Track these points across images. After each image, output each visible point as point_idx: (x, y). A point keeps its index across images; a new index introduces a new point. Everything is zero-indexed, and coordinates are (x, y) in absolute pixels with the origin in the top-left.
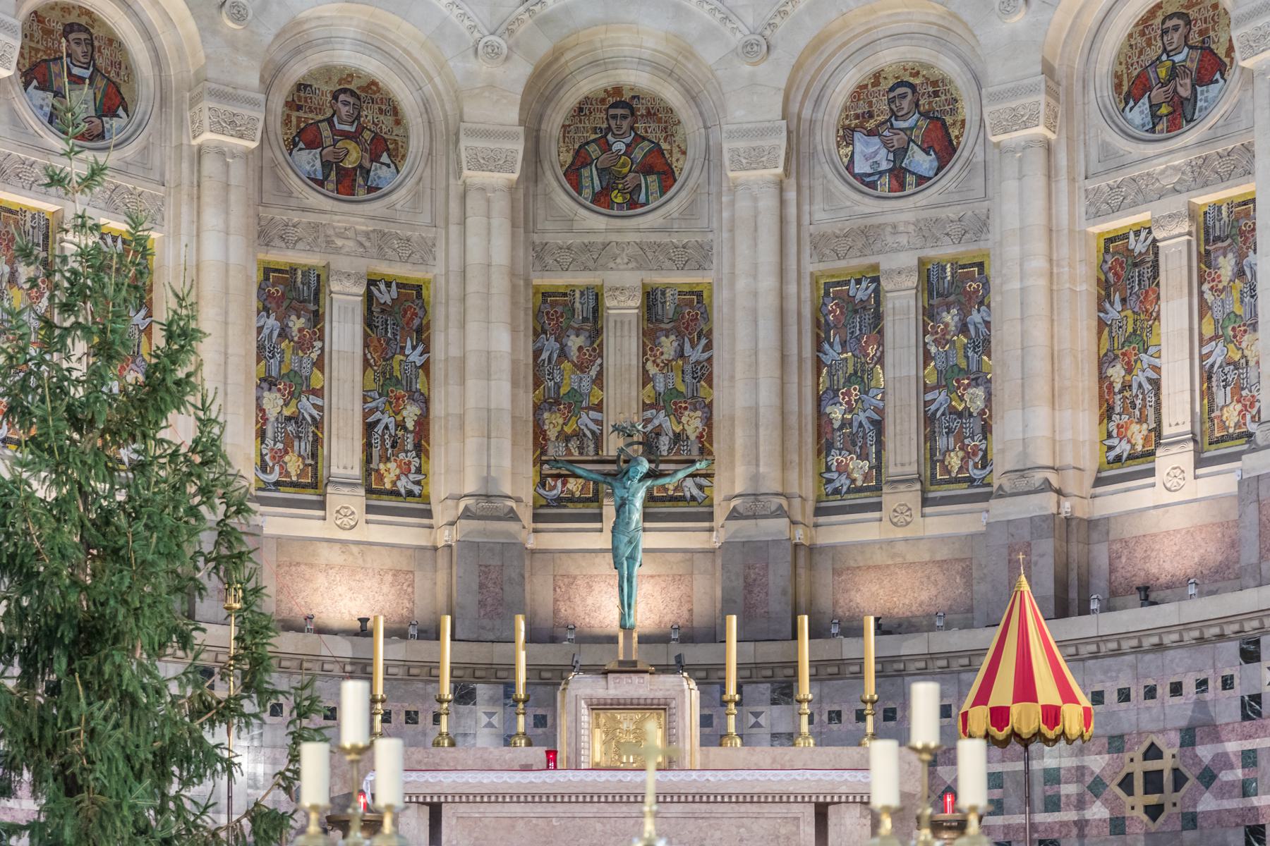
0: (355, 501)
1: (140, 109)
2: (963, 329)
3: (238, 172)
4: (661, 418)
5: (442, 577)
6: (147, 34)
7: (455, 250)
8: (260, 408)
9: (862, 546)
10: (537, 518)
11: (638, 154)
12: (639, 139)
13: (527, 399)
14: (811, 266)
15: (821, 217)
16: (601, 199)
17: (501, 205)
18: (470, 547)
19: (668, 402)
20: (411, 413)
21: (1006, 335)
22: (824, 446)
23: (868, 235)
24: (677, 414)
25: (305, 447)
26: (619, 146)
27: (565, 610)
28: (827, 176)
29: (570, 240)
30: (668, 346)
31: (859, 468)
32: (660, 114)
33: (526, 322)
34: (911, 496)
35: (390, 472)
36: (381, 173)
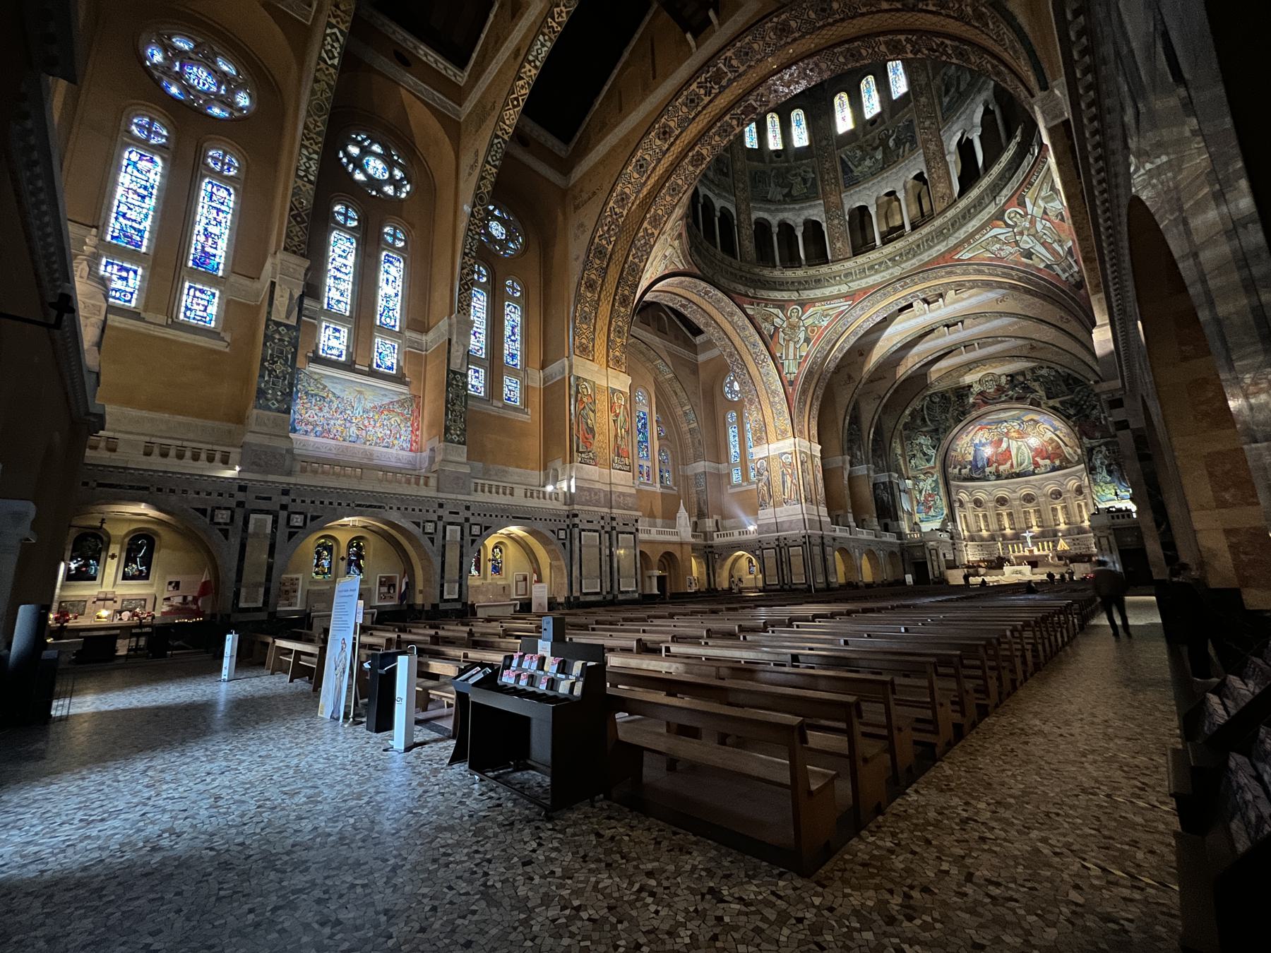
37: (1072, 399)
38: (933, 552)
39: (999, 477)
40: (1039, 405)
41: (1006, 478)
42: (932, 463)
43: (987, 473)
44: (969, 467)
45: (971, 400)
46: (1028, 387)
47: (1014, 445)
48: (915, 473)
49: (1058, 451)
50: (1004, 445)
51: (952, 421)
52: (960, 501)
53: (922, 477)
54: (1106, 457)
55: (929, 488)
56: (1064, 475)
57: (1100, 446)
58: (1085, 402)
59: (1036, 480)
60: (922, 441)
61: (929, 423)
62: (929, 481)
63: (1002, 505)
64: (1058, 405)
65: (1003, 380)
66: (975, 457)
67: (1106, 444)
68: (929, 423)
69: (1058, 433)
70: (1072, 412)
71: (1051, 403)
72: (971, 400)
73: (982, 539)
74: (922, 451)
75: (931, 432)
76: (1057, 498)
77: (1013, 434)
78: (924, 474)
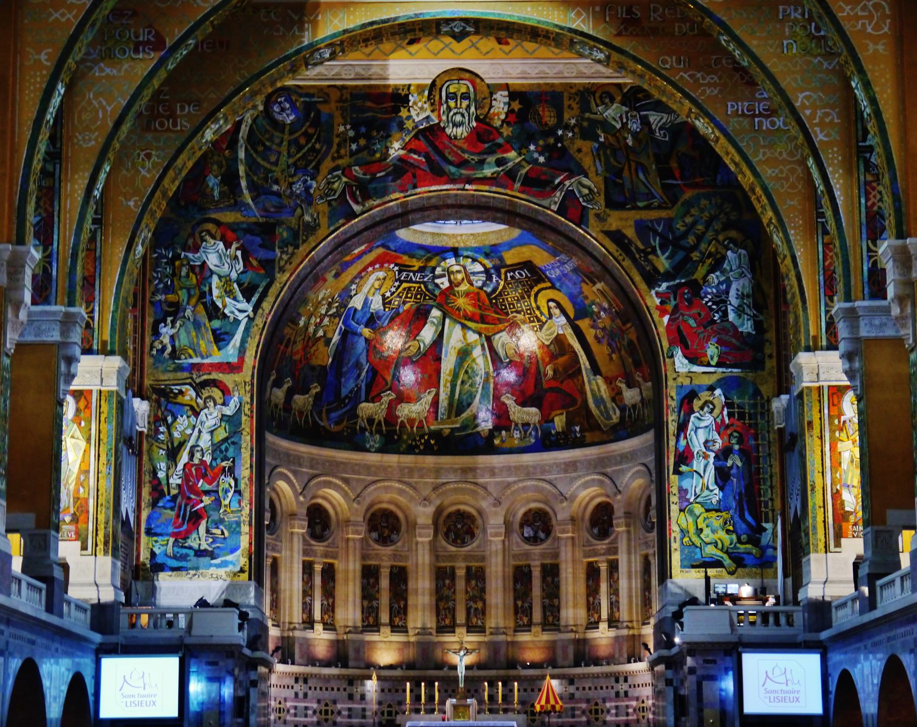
1: (332, 528)
2: (553, 582)
3: (358, 545)
4: (471, 604)
5: (411, 651)
7: (414, 558)
8: (362, 605)
9: (526, 642)
10: (437, 632)
11: (465, 528)
12: (465, 524)
14: (513, 563)
15: (516, 550)
17: (427, 547)
18: (418, 643)
19: (473, 599)
20: (402, 604)
22: (516, 613)
23: (527, 555)
24: (475, 602)
25: (374, 615)
26: (459, 526)
27: (445, 659)
28: (516, 537)
29: (446, 554)
31: (525, 620)
33: (434, 577)
34: (539, 629)
35: (397, 620)
36: (394, 537)
37: (669, 223)
40: (581, 220)
42: (230, 353)
45: (396, 149)
46: (564, 150)
49: (567, 386)
51: (322, 206)
54: (720, 428)
55: (206, 437)
56: (572, 466)
57: (711, 388)
58: (700, 238)
59: (492, 472)
60: (212, 260)
62: (211, 417)
63: (384, 540)
64: (630, 233)
65: (500, 105)
67: (726, 384)
68: (248, 198)
69: (584, 324)
70: (663, 262)
71: (616, 220)
72: (396, 149)
73: (312, 661)
74: (204, 296)
75: (250, 230)
78: (199, 387)
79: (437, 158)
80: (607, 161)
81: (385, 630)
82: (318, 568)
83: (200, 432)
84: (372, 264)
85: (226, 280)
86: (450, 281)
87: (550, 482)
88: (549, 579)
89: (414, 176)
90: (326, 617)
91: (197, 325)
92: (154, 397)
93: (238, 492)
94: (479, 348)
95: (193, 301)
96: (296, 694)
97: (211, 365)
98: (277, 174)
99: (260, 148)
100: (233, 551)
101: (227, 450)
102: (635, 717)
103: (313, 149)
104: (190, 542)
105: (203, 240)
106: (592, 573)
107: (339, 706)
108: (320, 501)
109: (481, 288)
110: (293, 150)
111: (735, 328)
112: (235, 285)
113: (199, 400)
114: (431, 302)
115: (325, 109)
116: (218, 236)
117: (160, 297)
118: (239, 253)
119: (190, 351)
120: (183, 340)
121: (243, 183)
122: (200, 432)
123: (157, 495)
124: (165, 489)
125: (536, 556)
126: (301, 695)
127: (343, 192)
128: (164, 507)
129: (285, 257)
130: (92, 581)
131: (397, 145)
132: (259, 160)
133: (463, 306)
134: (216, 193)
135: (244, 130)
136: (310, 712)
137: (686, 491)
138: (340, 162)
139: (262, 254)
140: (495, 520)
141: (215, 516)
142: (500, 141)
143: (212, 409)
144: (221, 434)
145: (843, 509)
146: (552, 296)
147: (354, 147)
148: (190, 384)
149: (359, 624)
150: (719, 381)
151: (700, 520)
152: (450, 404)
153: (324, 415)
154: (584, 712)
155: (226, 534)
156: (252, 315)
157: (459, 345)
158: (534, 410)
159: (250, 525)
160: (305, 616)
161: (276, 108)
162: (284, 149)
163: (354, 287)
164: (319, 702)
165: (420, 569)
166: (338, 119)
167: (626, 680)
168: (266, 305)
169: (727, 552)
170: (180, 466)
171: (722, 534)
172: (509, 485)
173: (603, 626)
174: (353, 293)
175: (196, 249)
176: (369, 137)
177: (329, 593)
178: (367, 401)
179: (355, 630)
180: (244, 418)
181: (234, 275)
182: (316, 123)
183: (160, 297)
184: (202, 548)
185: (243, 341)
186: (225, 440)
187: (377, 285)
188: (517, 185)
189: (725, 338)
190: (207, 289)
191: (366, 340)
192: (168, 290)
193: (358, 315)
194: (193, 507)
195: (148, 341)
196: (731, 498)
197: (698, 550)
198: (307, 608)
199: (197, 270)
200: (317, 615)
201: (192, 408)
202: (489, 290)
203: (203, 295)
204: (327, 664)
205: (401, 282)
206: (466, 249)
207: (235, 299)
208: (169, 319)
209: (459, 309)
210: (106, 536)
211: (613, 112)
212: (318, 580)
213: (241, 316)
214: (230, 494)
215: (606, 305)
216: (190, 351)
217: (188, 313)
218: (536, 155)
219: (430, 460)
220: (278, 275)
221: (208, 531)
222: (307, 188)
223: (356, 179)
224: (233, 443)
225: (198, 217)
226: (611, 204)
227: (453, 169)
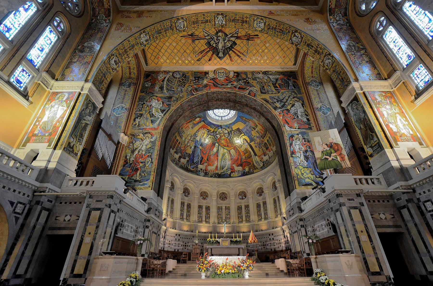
0: (205, 222)
6: (191, 189)
13: (217, 214)
16: (222, 200)
17: (215, 200)
18: (213, 226)
20: (209, 216)
21: (250, 210)
23: (241, 203)
30: (227, 210)
31: (241, 220)
32: (226, 194)
35: (207, 220)
38: (95, 214)
39: (206, 174)
41: (211, 177)
42: (155, 125)
43: (199, 169)
44: (187, 159)
45: (205, 82)
47: (222, 151)
48: (136, 131)
50: (215, 150)
52: (172, 184)
53: (141, 135)
55: (144, 147)
56: (251, 179)
60: (154, 104)
61: (165, 91)
62: (147, 141)
63: (204, 199)
66: (194, 152)
68: (165, 91)
71: (264, 96)
72: (205, 82)
75: (165, 98)
76: (242, 199)
77: (223, 142)
79: (215, 83)
80: (260, 84)
81: (204, 223)
82: (186, 204)
83: (143, 145)
84: (201, 127)
85: (157, 109)
86: (220, 136)
87: (245, 183)
88: (247, 209)
89: (210, 87)
90: (188, 218)
91: (147, 119)
92: (131, 136)
93: (152, 162)
94: (227, 153)
95: (147, 113)
96: (176, 239)
97: (149, 128)
98: (174, 87)
99: (170, 82)
100: (147, 180)
101: (150, 150)
102: (277, 246)
103: (184, 82)
104: (133, 178)
105: (152, 100)
106: (258, 206)
107: (189, 244)
108: (188, 187)
109: (227, 138)
110: (179, 82)
111: (302, 120)
112: (159, 110)
113: (144, 137)
114: (216, 142)
115: (187, 75)
116: (156, 99)
117: (138, 112)
118: (161, 103)
119: (144, 125)
120: (142, 122)
121: (165, 88)
122: (143, 145)
123: (125, 163)
124: (129, 162)
125: (243, 203)
126: (177, 240)
127: (191, 90)
128: (127, 167)
129: (174, 104)
130: (47, 158)
131: (205, 81)
132: (169, 84)
133: (223, 143)
134: (157, 90)
135: (166, 79)
136: (180, 245)
137: (296, 162)
138: (190, 84)
139: (168, 103)
140: (232, 193)
141: (143, 169)
142: (232, 80)
143: (147, 140)
144: (149, 146)
145: (393, 131)
146: (244, 138)
147: (194, 82)
148: (142, 133)
149: (197, 220)
150: (300, 132)
151: (302, 171)
152: (221, 167)
153: (189, 166)
154: (260, 246)
155: (146, 175)
156: (163, 116)
157: (223, 153)
158: (241, 167)
159: (154, 172)
160: (181, 217)
161: (175, 75)
162: (176, 82)
163: (197, 134)
164: (183, 242)
165: (213, 206)
166: (191, 76)
167: (272, 234)
168: (167, 114)
169: (313, 181)
170: (135, 155)
171: (310, 175)
172: (235, 185)
173: (263, 220)
174: (197, 136)
175: (150, 102)
176: (198, 80)
177: (188, 211)
178: (200, 164)
179: (195, 222)
180: (157, 142)
181: (159, 107)
182: (185, 77)
183: (138, 112)
184: (137, 179)
185: (159, 123)
186: (151, 147)
187: (203, 134)
188: (237, 89)
189: (299, 122)
190: (151, 111)
191: (200, 149)
192: (140, 111)
193: (198, 143)
194: (136, 167)
195: (131, 122)
196: (310, 164)
197: (303, 180)
198: (182, 215)
199: (149, 106)
200: (185, 217)
201: (141, 139)
202: (229, 138)
203: (150, 112)
204: (187, 231)
205: (209, 135)
206: (224, 125)
207: (159, 113)
208: (139, 117)
209: (222, 143)
210: (63, 142)
211: (260, 76)
212: (186, 207)
213: (160, 117)
214: (149, 163)
215: (258, 135)
216: (144, 125)
217: (145, 116)
218: (241, 83)
219: (216, 179)
220: (171, 107)
221: (140, 174)
222: (181, 90)
223: (195, 88)
224: (152, 148)
225: (151, 95)
226: (262, 93)
227: (220, 86)
